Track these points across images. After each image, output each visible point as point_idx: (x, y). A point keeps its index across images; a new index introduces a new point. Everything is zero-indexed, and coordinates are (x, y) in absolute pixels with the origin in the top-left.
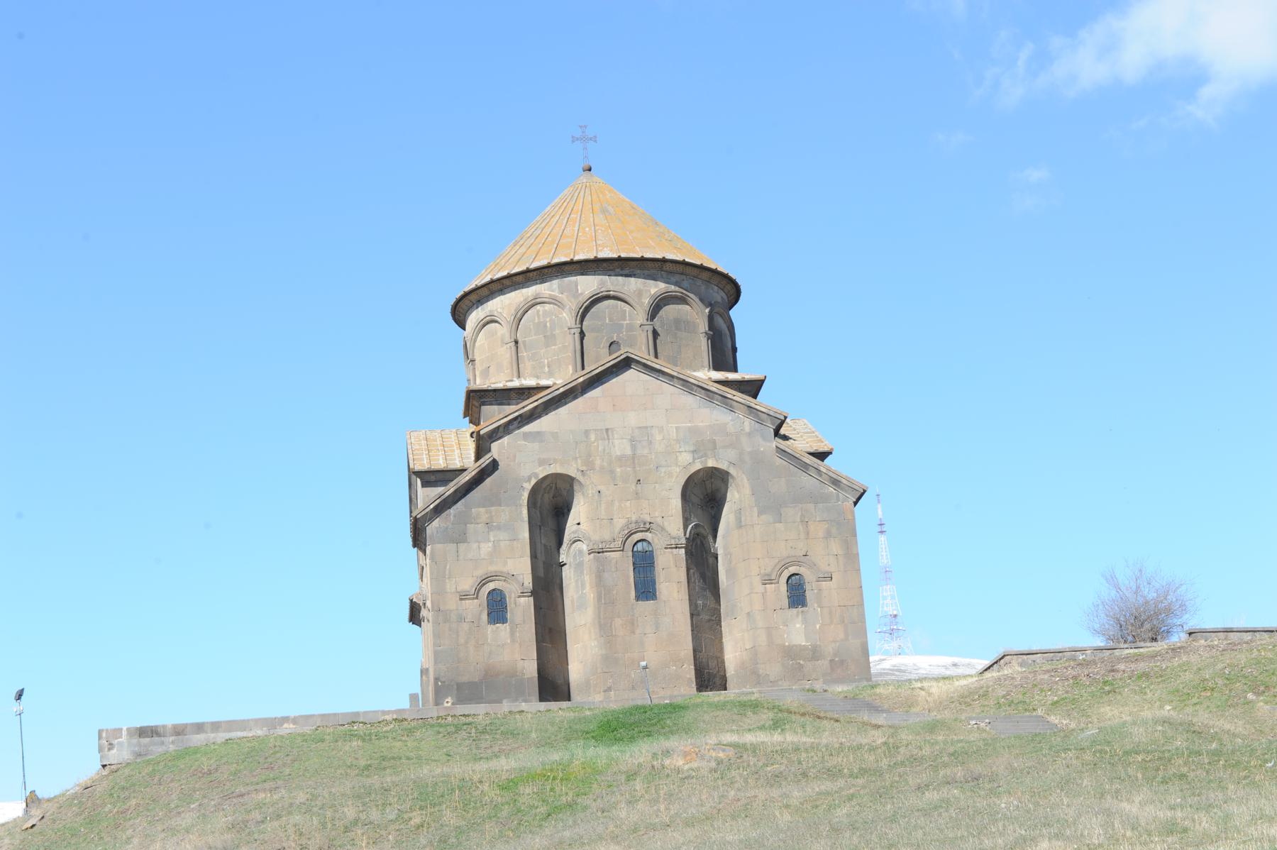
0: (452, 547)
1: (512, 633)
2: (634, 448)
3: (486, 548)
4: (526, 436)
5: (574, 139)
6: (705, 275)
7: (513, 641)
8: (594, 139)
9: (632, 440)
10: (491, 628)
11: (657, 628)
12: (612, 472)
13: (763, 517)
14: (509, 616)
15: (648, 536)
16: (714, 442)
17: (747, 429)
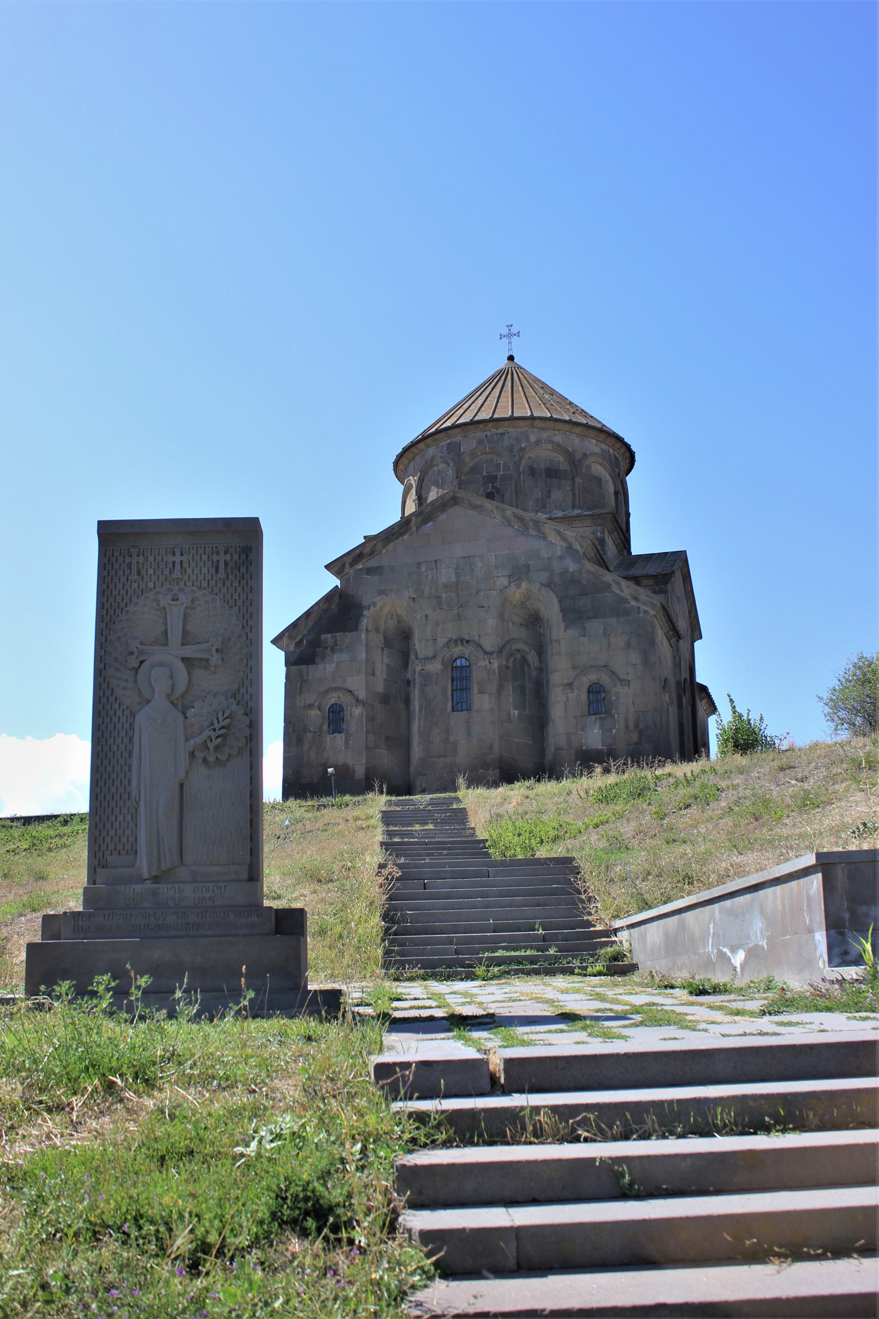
0: (303, 667)
1: (347, 741)
2: (458, 575)
3: (330, 667)
4: (369, 571)
5: (501, 337)
6: (578, 430)
7: (347, 748)
8: (518, 334)
9: (457, 567)
10: (329, 738)
11: (469, 735)
12: (439, 597)
13: (569, 632)
14: (344, 726)
15: (467, 653)
16: (528, 567)
17: (559, 553)
